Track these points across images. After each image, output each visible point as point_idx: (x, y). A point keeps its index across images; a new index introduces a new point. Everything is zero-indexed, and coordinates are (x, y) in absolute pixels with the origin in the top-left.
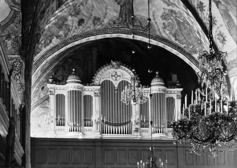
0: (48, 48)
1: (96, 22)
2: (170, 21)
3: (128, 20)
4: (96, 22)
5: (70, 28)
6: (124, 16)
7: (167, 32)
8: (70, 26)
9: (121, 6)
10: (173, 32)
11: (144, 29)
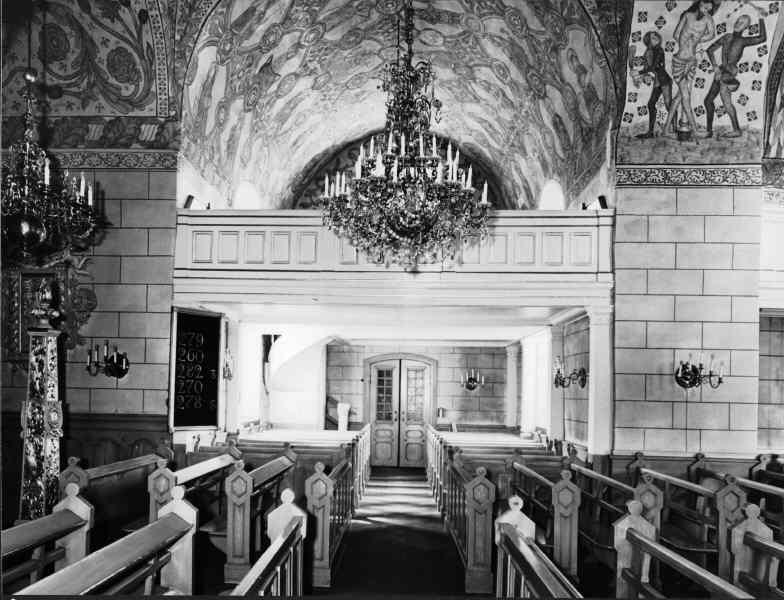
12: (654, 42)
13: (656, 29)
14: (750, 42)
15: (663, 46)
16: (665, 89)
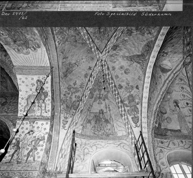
0: (140, 112)
2: (145, 30)
5: (138, 95)
6: (140, 61)
8: (136, 95)
11: (150, 50)
12: (18, 140)
13: (19, 137)
14: (41, 140)
15: (20, 141)
16: (18, 150)
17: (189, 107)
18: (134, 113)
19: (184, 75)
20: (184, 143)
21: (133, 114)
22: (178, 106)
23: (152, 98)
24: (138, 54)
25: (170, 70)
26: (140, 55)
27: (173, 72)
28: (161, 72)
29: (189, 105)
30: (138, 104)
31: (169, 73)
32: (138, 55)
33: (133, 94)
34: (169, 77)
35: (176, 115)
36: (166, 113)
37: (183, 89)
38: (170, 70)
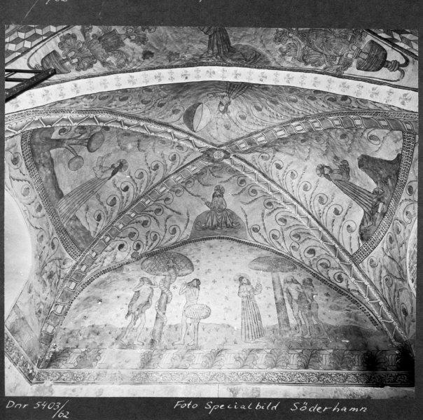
1: (172, 57)
2: (289, 42)
3: (222, 53)
4: (172, 57)
5: (129, 59)
6: (216, 48)
7: (290, 59)
9: (210, 37)
10: (299, 54)
17: (119, 195)
18: (72, 58)
19: (184, 160)
20: (39, 214)
21: (70, 55)
22: (113, 174)
23: (125, 103)
24: (231, 39)
25: (191, 128)
26: (229, 43)
27: (191, 135)
28: (186, 109)
29: (125, 194)
30: (104, 63)
31: (186, 129)
32: (228, 40)
33: (124, 45)
34: (178, 130)
35: (92, 176)
36: (90, 151)
37: (154, 170)
38: (191, 128)
